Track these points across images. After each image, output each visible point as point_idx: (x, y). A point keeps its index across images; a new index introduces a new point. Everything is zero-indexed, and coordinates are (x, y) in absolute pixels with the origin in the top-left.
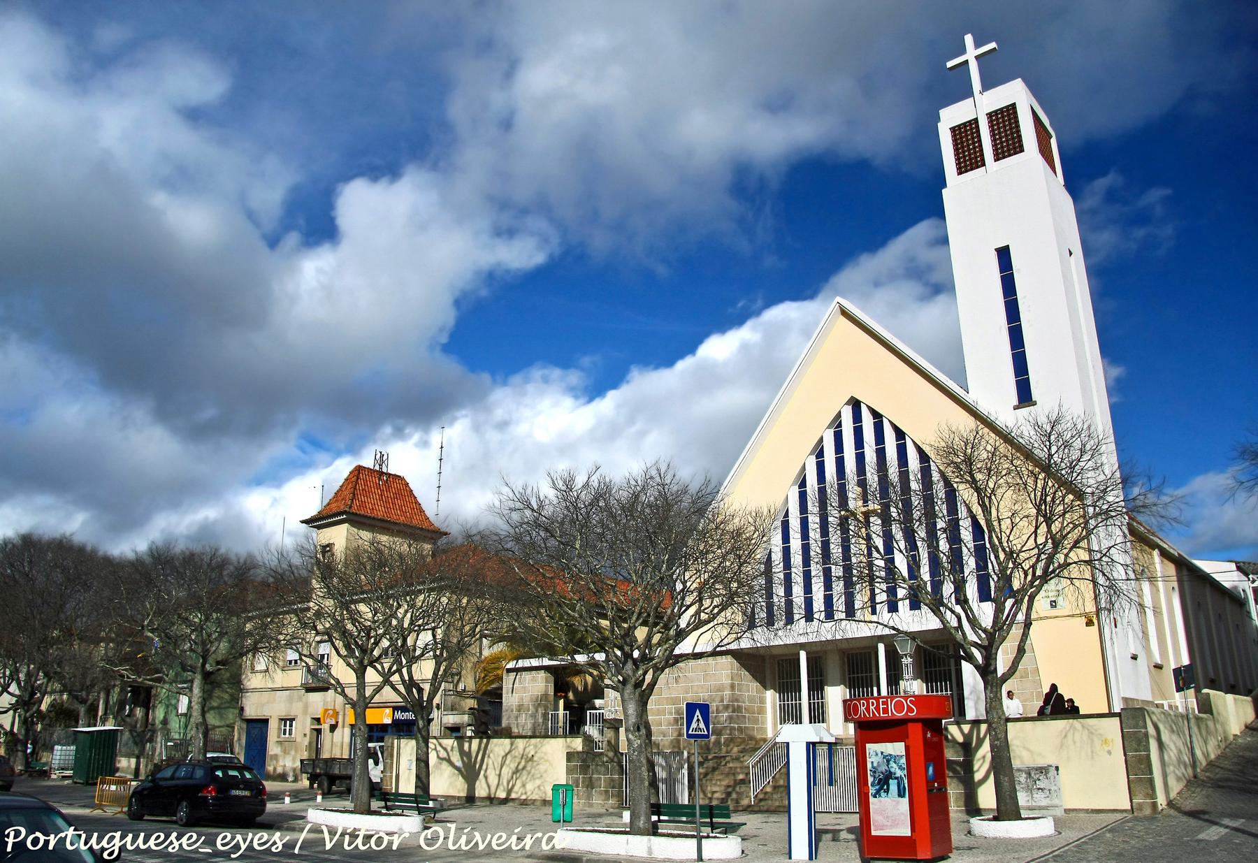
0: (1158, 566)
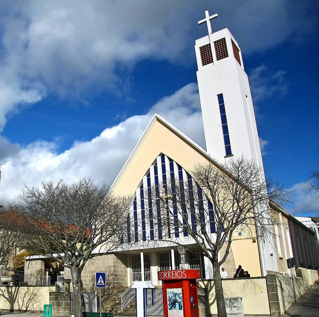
0: (281, 219)
